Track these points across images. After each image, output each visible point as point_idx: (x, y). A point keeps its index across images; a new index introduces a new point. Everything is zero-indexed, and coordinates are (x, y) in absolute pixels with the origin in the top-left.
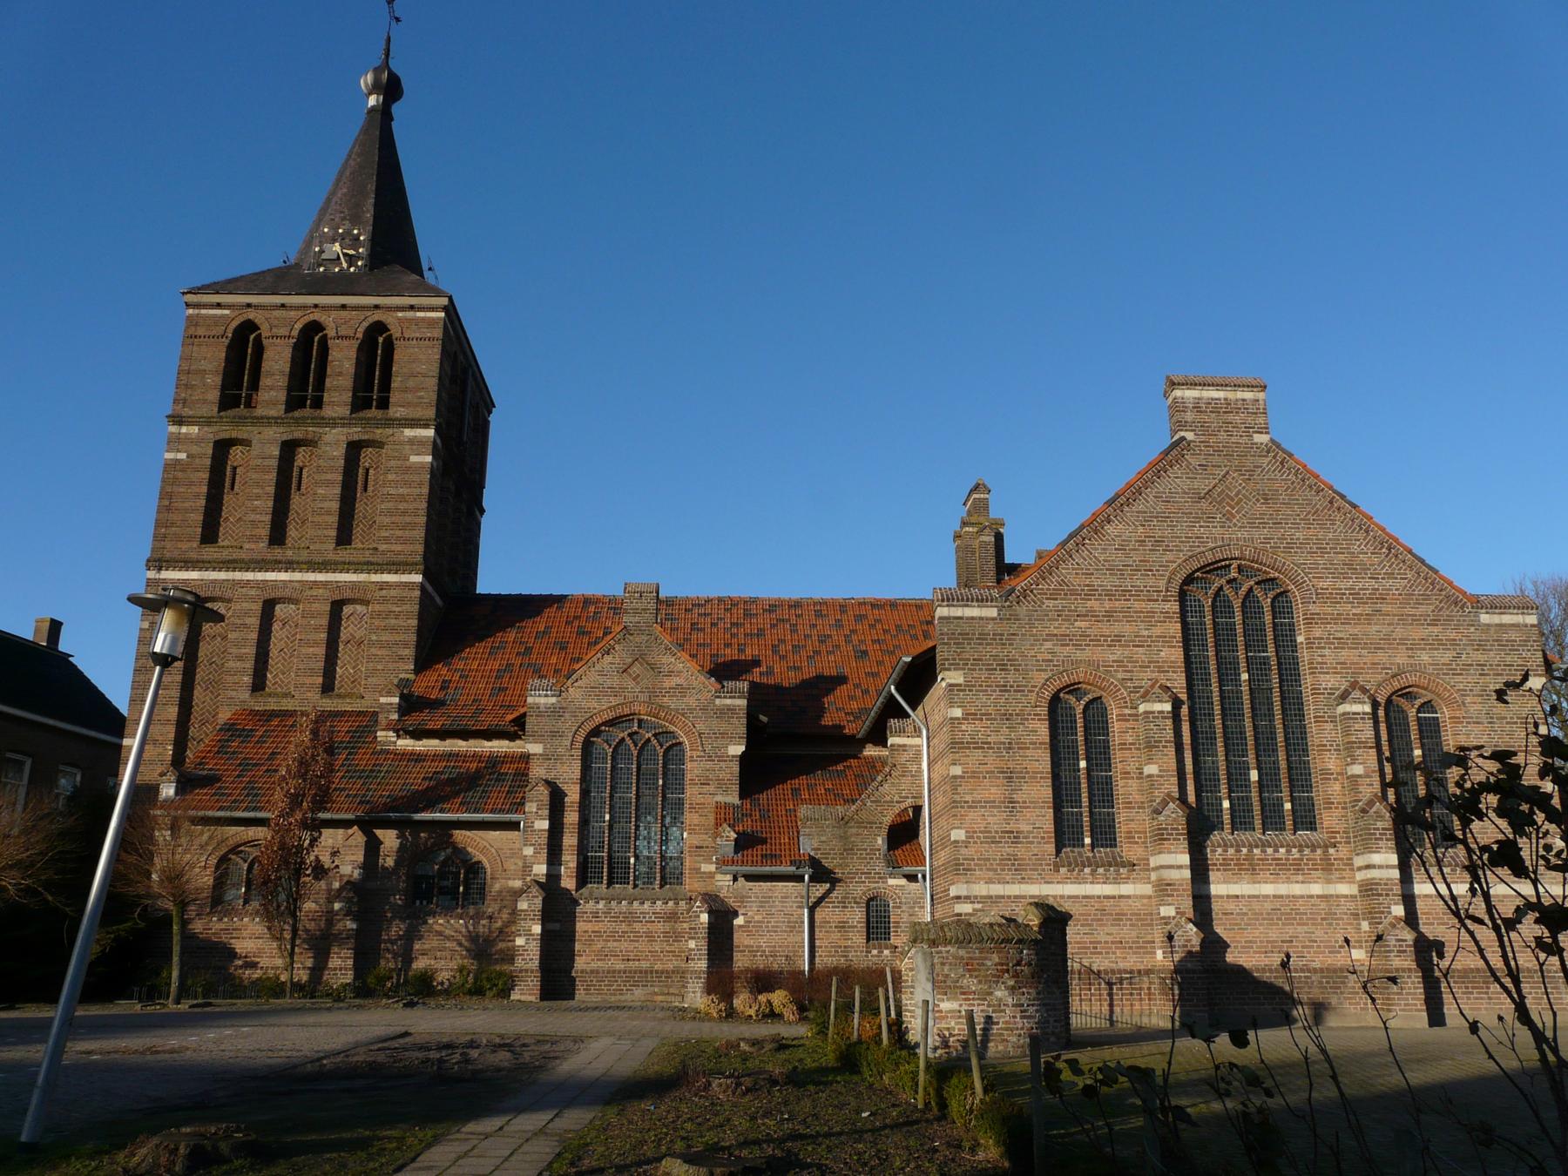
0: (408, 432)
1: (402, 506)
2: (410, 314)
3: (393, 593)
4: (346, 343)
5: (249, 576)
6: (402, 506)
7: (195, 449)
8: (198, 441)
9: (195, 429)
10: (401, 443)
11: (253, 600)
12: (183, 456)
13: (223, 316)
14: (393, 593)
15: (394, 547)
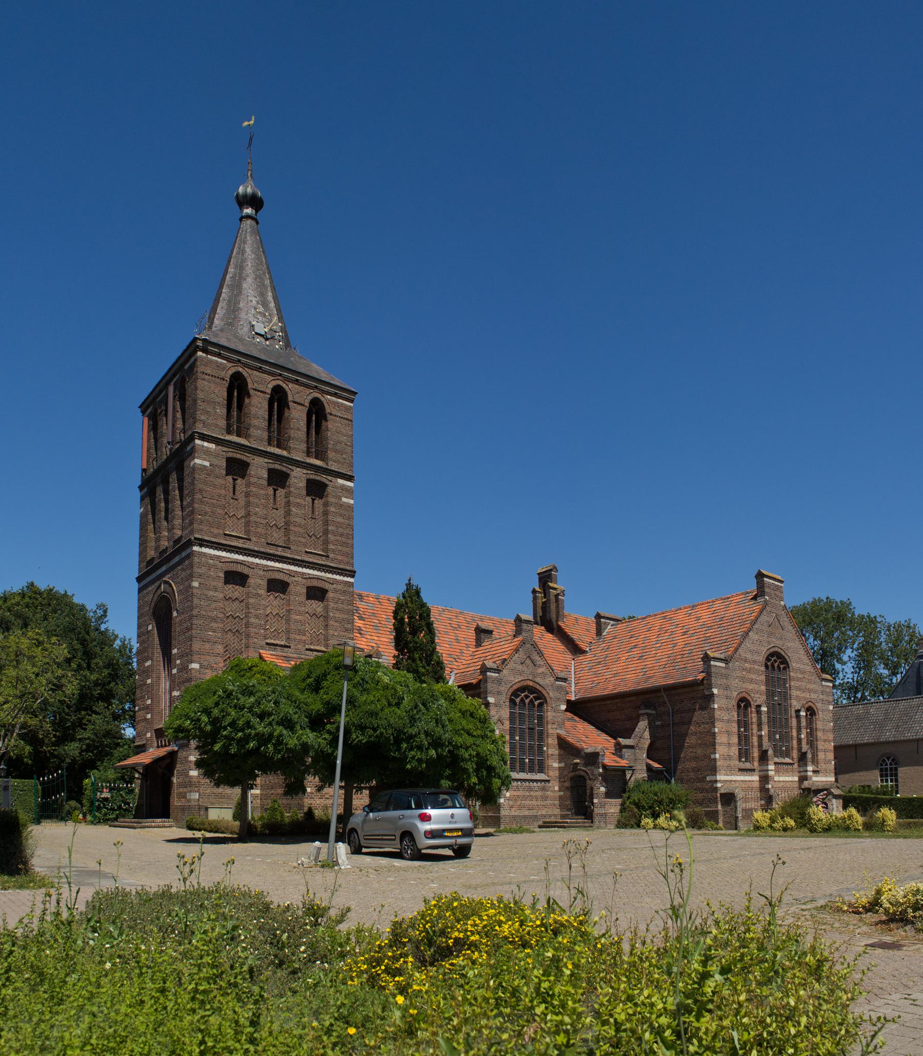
0: (340, 481)
1: (340, 530)
2: (334, 399)
3: (339, 587)
4: (300, 407)
5: (257, 561)
6: (340, 530)
7: (216, 462)
8: (217, 456)
9: (212, 446)
10: (336, 487)
11: (261, 578)
12: (207, 464)
13: (221, 363)
14: (339, 587)
15: (338, 557)
